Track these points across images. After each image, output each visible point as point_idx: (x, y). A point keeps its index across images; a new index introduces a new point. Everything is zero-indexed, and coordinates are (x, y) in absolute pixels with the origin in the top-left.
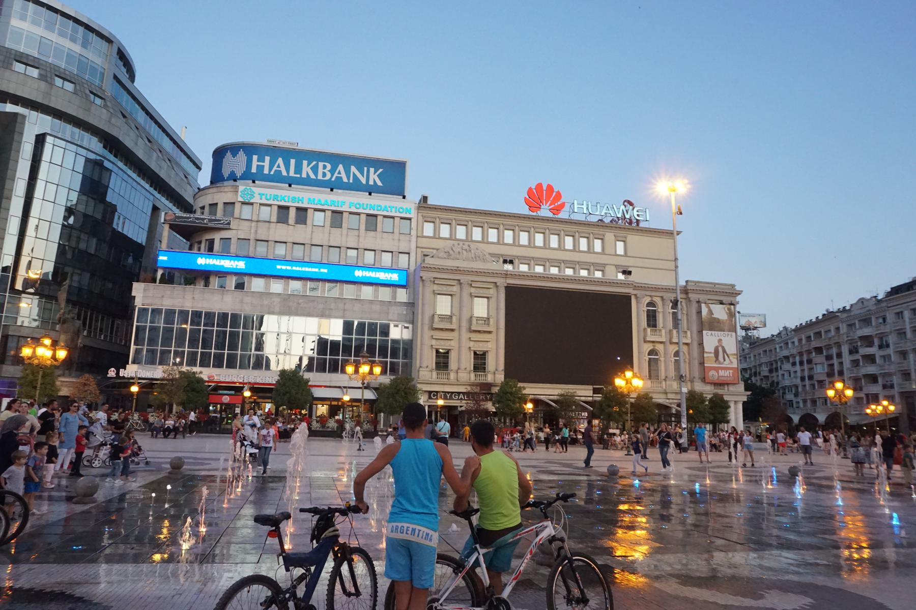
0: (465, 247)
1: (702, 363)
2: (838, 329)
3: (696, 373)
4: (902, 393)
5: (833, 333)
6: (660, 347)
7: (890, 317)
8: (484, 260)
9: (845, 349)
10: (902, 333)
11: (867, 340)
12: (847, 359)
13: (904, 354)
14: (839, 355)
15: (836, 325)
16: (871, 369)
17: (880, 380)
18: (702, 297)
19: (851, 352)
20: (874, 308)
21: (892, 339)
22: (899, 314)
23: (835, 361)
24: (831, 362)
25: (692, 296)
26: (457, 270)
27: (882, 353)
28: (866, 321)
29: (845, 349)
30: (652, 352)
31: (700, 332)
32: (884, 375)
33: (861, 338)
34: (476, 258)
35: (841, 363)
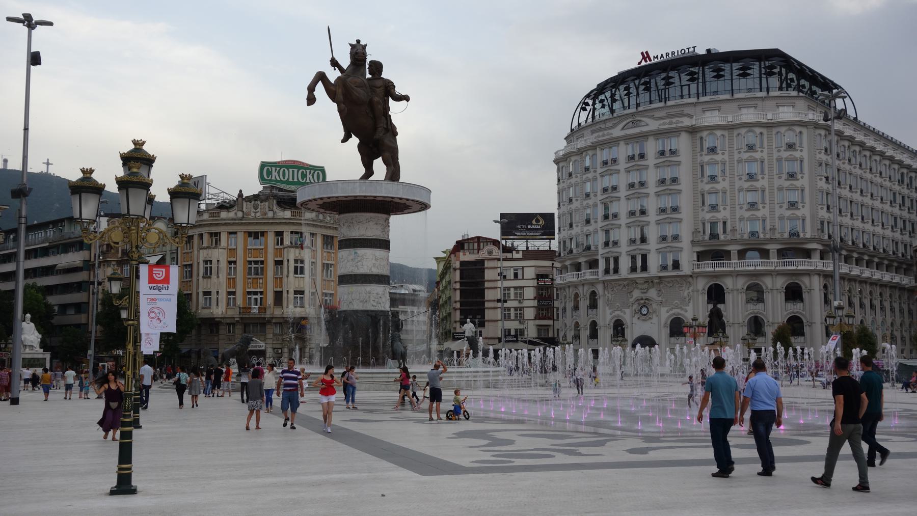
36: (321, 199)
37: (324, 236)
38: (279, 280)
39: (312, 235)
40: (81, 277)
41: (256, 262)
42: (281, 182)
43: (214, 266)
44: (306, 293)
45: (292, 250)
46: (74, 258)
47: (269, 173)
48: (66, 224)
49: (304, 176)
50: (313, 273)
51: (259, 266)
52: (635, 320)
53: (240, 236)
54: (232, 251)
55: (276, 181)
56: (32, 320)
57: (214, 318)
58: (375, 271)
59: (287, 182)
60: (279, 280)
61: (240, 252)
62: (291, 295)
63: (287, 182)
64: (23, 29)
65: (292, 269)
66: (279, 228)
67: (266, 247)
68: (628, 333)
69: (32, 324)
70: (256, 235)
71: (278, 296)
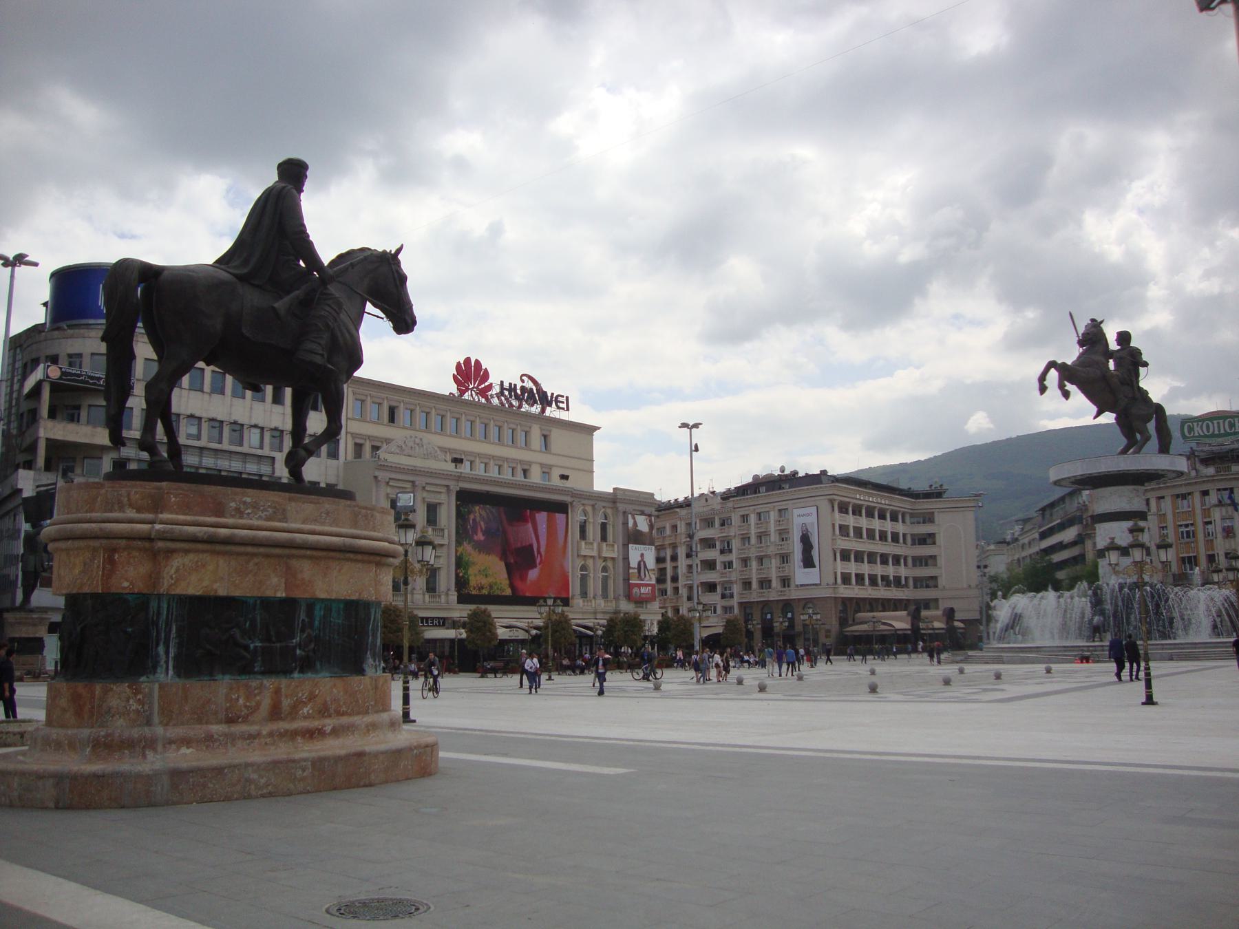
0: (417, 441)
1: (627, 579)
2: (675, 527)
3: (621, 592)
4: (741, 604)
5: (668, 532)
6: (590, 562)
7: (736, 519)
8: (436, 458)
9: (682, 551)
10: (745, 538)
11: (708, 543)
12: (683, 562)
13: (745, 561)
14: (674, 558)
15: (673, 522)
16: (711, 577)
17: (719, 588)
18: (629, 508)
19: (688, 556)
20: (719, 507)
21: (735, 544)
22: (745, 518)
23: (669, 565)
24: (662, 566)
25: (621, 507)
26: (414, 471)
27: (726, 558)
28: (709, 523)
29: (682, 551)
30: (584, 568)
31: (626, 546)
32: (723, 584)
33: (703, 541)
34: (427, 456)
35: (675, 568)
38: (1209, 543)
40: (1075, 552)
41: (1187, 526)
42: (1206, 436)
45: (1217, 509)
46: (1070, 534)
47: (1191, 429)
48: (1067, 500)
49: (1232, 425)
51: (1191, 528)
53: (1168, 501)
54: (1162, 517)
55: (1200, 436)
59: (1213, 436)
60: (1209, 543)
61: (1170, 517)
63: (1213, 436)
64: (686, 430)
66: (1205, 487)
67: (1194, 510)
70: (1184, 496)
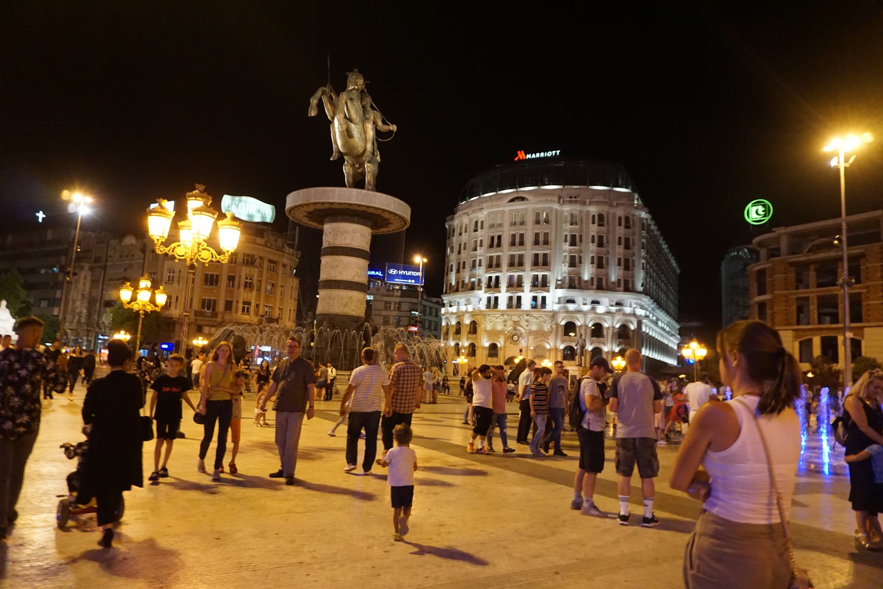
36: (315, 204)
37: (270, 261)
39: (261, 258)
43: (176, 275)
44: (253, 304)
45: (244, 268)
50: (259, 290)
52: (508, 344)
56: (7, 307)
57: (172, 318)
58: (356, 279)
62: (241, 306)
65: (243, 283)
68: (501, 353)
69: (8, 311)
71: (229, 305)
